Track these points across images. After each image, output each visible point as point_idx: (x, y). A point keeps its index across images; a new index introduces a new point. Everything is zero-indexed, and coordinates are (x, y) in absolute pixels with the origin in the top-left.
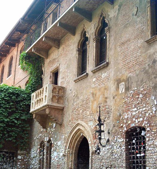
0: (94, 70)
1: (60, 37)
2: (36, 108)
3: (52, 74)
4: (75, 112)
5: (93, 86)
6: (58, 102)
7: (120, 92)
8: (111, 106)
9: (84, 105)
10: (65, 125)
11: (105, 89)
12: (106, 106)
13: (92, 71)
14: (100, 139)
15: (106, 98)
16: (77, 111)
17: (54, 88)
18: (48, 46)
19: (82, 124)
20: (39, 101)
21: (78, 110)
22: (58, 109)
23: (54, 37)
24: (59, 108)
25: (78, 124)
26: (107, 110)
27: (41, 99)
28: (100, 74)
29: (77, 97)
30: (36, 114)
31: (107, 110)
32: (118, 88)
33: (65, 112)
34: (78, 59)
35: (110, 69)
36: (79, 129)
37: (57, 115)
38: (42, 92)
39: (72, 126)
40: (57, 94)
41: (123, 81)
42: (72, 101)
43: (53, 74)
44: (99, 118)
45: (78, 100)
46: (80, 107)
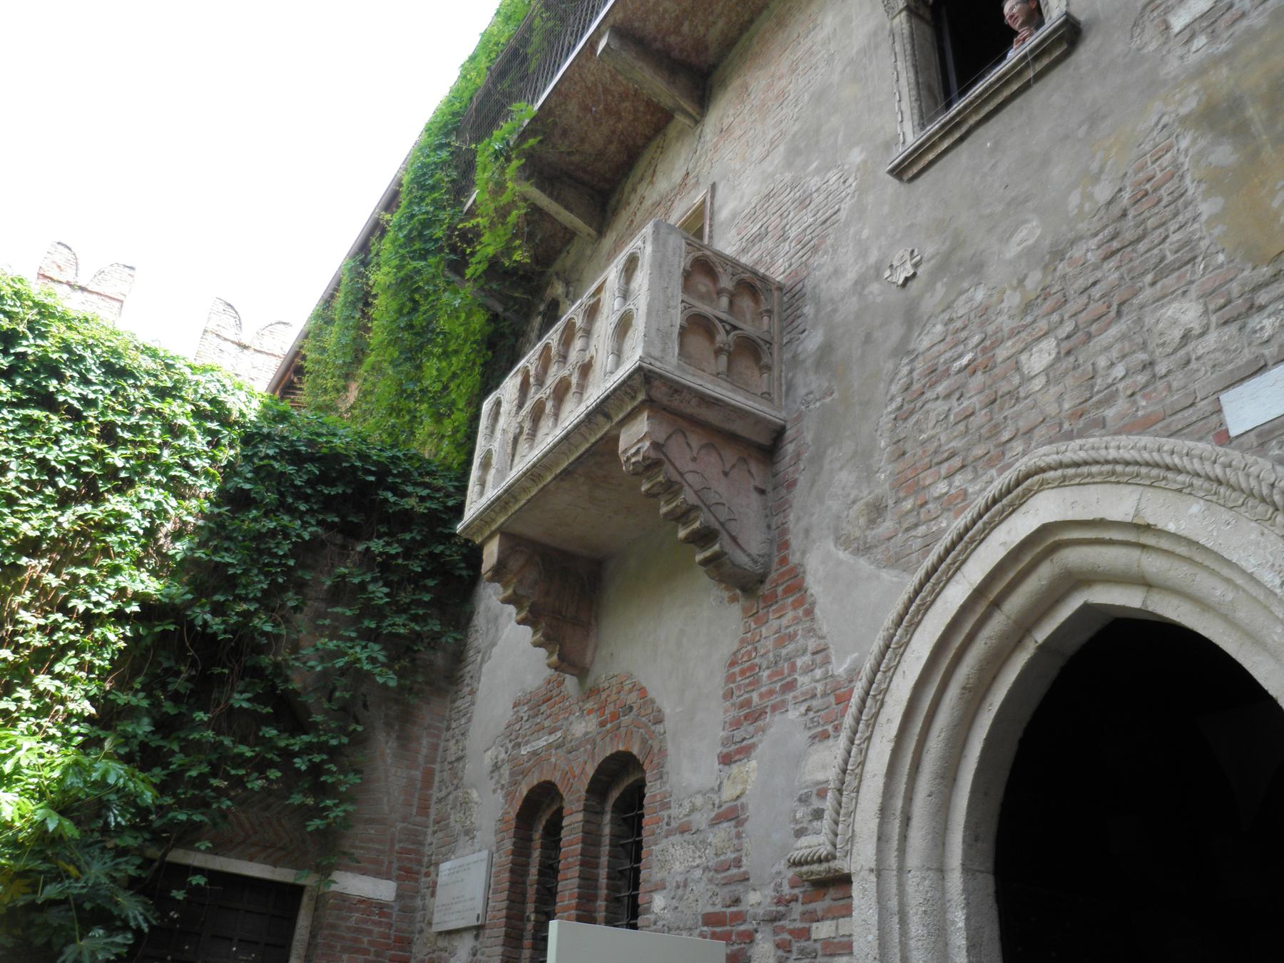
1: (714, 35)
4: (941, 406)
6: (729, 375)
9: (1080, 283)
18: (613, 148)
21: (987, 369)
22: (732, 438)
23: (672, 39)
24: (738, 427)
30: (513, 541)
33: (798, 456)
34: (912, 39)
37: (721, 489)
39: (918, 543)
40: (724, 316)
42: (896, 331)
45: (966, 285)
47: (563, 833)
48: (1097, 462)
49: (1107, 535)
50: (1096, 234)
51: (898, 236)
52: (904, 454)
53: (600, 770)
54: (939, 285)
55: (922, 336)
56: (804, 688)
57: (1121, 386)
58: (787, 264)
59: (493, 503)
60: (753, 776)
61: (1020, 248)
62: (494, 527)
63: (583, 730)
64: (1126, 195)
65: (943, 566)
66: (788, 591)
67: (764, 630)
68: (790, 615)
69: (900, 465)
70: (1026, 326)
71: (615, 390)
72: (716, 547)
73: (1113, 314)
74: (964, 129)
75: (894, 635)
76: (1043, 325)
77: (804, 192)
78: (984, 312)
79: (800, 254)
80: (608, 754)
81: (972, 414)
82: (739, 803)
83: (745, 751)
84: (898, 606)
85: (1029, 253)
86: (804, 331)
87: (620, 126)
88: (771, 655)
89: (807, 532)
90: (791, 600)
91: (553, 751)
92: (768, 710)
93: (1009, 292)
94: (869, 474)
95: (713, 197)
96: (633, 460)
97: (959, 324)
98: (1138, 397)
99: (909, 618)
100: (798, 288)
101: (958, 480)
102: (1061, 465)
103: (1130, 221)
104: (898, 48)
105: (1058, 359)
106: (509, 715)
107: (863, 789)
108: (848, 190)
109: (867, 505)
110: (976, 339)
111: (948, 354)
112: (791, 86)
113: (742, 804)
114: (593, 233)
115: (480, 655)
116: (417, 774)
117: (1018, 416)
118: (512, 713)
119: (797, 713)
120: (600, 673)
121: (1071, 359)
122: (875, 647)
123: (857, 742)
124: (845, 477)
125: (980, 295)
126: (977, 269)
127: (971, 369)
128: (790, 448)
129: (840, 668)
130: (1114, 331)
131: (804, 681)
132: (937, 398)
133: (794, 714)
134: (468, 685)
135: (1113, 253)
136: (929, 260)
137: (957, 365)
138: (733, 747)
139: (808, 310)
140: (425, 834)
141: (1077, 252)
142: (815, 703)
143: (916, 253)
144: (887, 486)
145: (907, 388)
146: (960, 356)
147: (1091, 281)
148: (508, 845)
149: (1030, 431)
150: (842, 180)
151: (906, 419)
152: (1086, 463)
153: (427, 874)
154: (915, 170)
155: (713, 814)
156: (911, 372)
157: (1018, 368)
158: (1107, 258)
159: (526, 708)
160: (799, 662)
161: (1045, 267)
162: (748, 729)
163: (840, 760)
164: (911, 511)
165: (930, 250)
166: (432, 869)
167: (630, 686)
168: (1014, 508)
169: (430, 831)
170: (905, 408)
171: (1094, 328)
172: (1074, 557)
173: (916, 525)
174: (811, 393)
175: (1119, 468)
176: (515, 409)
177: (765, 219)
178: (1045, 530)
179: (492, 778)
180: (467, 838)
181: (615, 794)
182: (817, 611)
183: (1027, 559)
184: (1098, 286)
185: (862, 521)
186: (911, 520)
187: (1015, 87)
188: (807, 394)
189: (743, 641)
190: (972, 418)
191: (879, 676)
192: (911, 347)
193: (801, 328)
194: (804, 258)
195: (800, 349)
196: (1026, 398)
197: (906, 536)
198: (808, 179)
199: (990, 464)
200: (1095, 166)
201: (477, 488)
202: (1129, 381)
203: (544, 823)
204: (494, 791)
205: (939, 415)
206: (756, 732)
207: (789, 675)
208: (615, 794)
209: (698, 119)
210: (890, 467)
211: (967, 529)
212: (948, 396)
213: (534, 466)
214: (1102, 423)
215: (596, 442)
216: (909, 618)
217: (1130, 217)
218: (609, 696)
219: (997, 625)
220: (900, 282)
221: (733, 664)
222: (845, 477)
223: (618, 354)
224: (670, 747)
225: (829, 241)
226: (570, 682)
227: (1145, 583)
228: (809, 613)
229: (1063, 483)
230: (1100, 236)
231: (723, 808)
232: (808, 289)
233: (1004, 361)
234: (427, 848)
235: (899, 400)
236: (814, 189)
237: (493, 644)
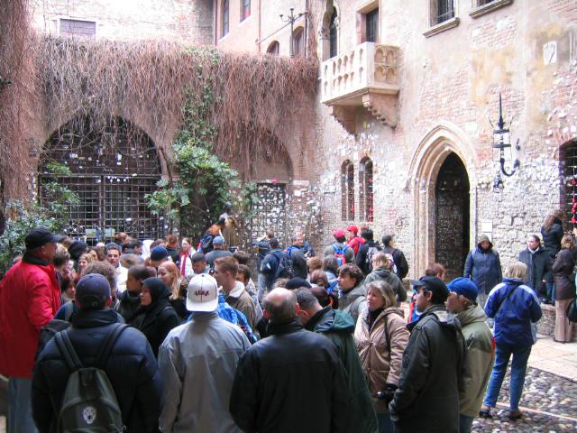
0: (474, 13)
3: (359, 16)
5: (474, 46)
6: (387, 80)
7: (546, 62)
8: (523, 92)
9: (452, 88)
10: (405, 129)
11: (506, 54)
12: (509, 90)
13: (470, 15)
14: (502, 161)
15: (510, 74)
17: (379, 51)
20: (343, 79)
24: (390, 92)
25: (439, 128)
26: (511, 99)
27: (350, 76)
28: (491, 21)
29: (432, 68)
30: (336, 107)
31: (511, 99)
32: (539, 52)
35: (517, 10)
36: (441, 139)
38: (349, 59)
41: (554, 37)
44: (501, 119)
78: (437, 84)
128: (401, 96)
130: (456, 101)
178: (441, 137)
214: (451, 120)
216: (421, 145)
226: (352, 137)
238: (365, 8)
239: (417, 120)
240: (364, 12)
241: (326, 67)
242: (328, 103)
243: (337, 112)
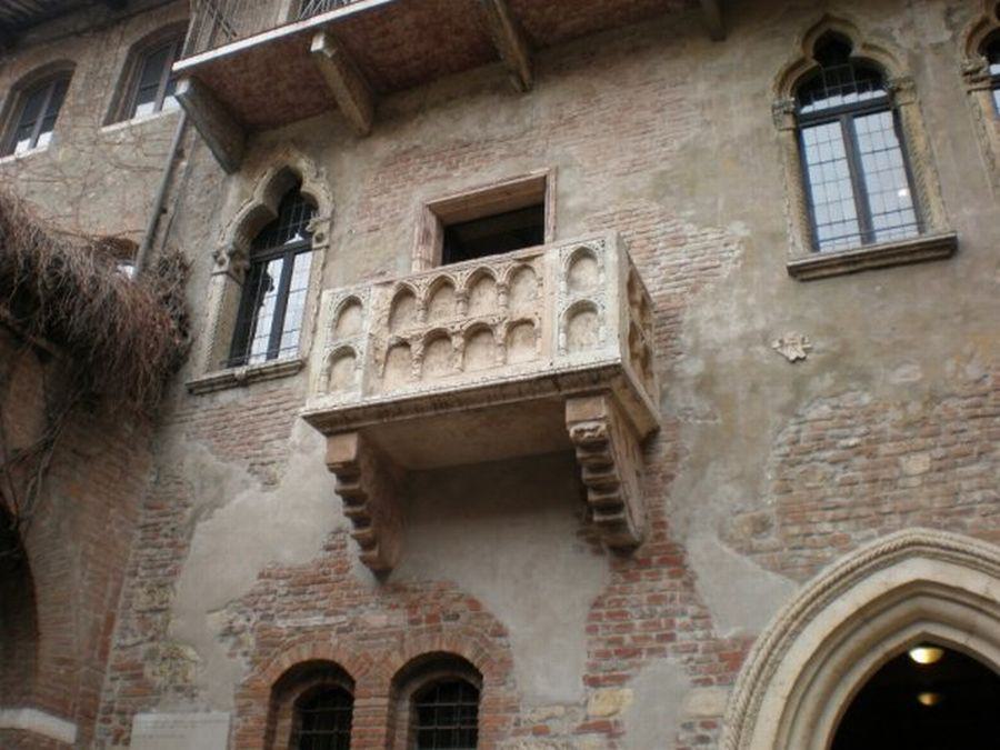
2: (400, 385)
3: (432, 222)
4: (831, 469)
9: (952, 426)
16: (861, 461)
18: (415, 63)
19: (977, 551)
20: (457, 342)
21: (871, 455)
23: (533, 12)
24: (638, 421)
27: (501, 331)
30: (366, 444)
33: (675, 457)
39: (802, 561)
42: (784, 396)
43: (437, 224)
45: (853, 385)
46: (891, 431)
47: (355, 712)
48: (964, 552)
49: (959, 597)
50: (965, 398)
51: (788, 319)
52: (790, 491)
53: (412, 662)
54: (828, 375)
55: (810, 409)
56: (684, 643)
57: (978, 506)
58: (657, 287)
59: (370, 406)
60: (629, 702)
61: (904, 380)
62: (354, 425)
63: (385, 623)
64: (989, 383)
65: (835, 587)
66: (664, 562)
67: (635, 586)
68: (665, 582)
69: (784, 498)
70: (906, 438)
71: (583, 371)
72: (622, 516)
73: (975, 456)
74: (859, 266)
75: (790, 625)
76: (920, 442)
77: (677, 231)
78: (870, 415)
79: (674, 283)
80: (427, 649)
81: (857, 483)
82: (612, 719)
83: (620, 680)
84: (798, 607)
85: (913, 387)
86: (680, 353)
87: (436, 52)
88: (645, 608)
89: (688, 521)
90: (665, 570)
91: (333, 633)
92: (645, 652)
93: (892, 409)
94: (756, 496)
95: (556, 179)
96: (587, 434)
97: (844, 412)
98: (989, 517)
99: (804, 616)
100: (673, 312)
101: (842, 526)
102: (937, 546)
103: (990, 400)
104: (785, 159)
105: (931, 470)
106: (253, 583)
107: (758, 728)
108: (730, 254)
109: (752, 518)
110: (862, 430)
111: (836, 432)
112: (656, 122)
113: (616, 723)
114: (366, 128)
115: (190, 509)
116: (102, 618)
117: (894, 499)
118: (257, 582)
119: (678, 660)
120: (402, 573)
121: (942, 475)
122: (769, 629)
123: (755, 694)
124: (729, 493)
125: (866, 399)
126: (865, 378)
127: (856, 450)
128: (664, 448)
129: (725, 633)
130: (975, 468)
131: (683, 637)
132: (823, 461)
133: (672, 660)
134: (166, 536)
135: (977, 417)
136: (818, 352)
137: (843, 442)
138: (601, 675)
139: (687, 339)
140: (102, 680)
141: (952, 403)
142: (696, 656)
143: (806, 341)
144: (774, 510)
145: (794, 443)
146: (846, 437)
147: (960, 428)
148: (260, 710)
149: (905, 513)
150: (723, 242)
151: (792, 466)
152: (957, 550)
153: (106, 721)
154: (811, 275)
155: (576, 725)
156: (798, 432)
157: (897, 465)
158: (976, 417)
159: (282, 582)
160: (678, 621)
161: (925, 404)
162: (614, 662)
163: (740, 705)
164: (798, 535)
165: (820, 345)
166: (113, 716)
167: (456, 596)
168: (894, 561)
169: (107, 677)
170: (792, 457)
171: (960, 460)
172: (926, 603)
173: (801, 548)
174: (691, 409)
175: (980, 561)
176: (386, 320)
177: (627, 233)
179: (222, 641)
180: (180, 695)
181: (415, 686)
182: (697, 584)
183: (898, 597)
184: (965, 434)
185: (746, 529)
186: (797, 542)
187: (906, 259)
188: (685, 409)
189: (610, 590)
190: (856, 487)
191: (776, 652)
192: (800, 413)
193: (678, 348)
194: (678, 290)
195: (677, 367)
196: (904, 488)
197: (792, 553)
198: (683, 221)
199: (872, 524)
200: (967, 350)
201: (324, 379)
202: (983, 505)
203: (298, 695)
204: (231, 655)
205: (825, 473)
206: (632, 665)
207: (667, 628)
208: (415, 686)
209: (526, 89)
210: (776, 498)
211: (859, 566)
212: (834, 463)
213: (449, 394)
214: (961, 527)
215: (532, 401)
217: (992, 396)
218: (422, 598)
219: (866, 633)
220: (792, 357)
221: (597, 604)
222: (729, 493)
223: (567, 331)
224: (517, 659)
225: (709, 287)
226: (360, 574)
227: (971, 630)
228: (689, 585)
229: (934, 557)
230: (969, 401)
231: (591, 721)
232: (686, 317)
233: (886, 455)
234: (103, 694)
235: (787, 449)
236: (690, 234)
237: (216, 506)
238: (466, 200)
239: (762, 525)
240: (450, 221)
241: (352, 302)
242: (330, 424)
243: (363, 464)
